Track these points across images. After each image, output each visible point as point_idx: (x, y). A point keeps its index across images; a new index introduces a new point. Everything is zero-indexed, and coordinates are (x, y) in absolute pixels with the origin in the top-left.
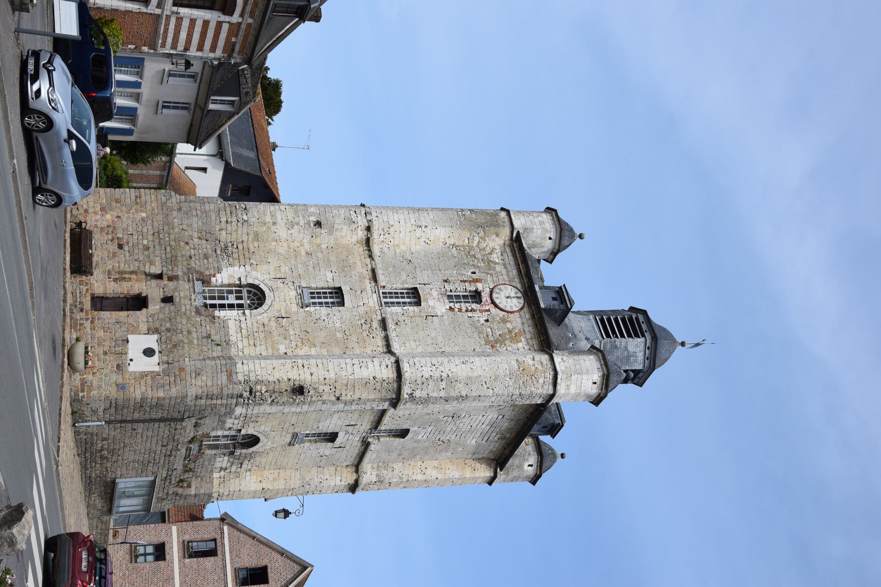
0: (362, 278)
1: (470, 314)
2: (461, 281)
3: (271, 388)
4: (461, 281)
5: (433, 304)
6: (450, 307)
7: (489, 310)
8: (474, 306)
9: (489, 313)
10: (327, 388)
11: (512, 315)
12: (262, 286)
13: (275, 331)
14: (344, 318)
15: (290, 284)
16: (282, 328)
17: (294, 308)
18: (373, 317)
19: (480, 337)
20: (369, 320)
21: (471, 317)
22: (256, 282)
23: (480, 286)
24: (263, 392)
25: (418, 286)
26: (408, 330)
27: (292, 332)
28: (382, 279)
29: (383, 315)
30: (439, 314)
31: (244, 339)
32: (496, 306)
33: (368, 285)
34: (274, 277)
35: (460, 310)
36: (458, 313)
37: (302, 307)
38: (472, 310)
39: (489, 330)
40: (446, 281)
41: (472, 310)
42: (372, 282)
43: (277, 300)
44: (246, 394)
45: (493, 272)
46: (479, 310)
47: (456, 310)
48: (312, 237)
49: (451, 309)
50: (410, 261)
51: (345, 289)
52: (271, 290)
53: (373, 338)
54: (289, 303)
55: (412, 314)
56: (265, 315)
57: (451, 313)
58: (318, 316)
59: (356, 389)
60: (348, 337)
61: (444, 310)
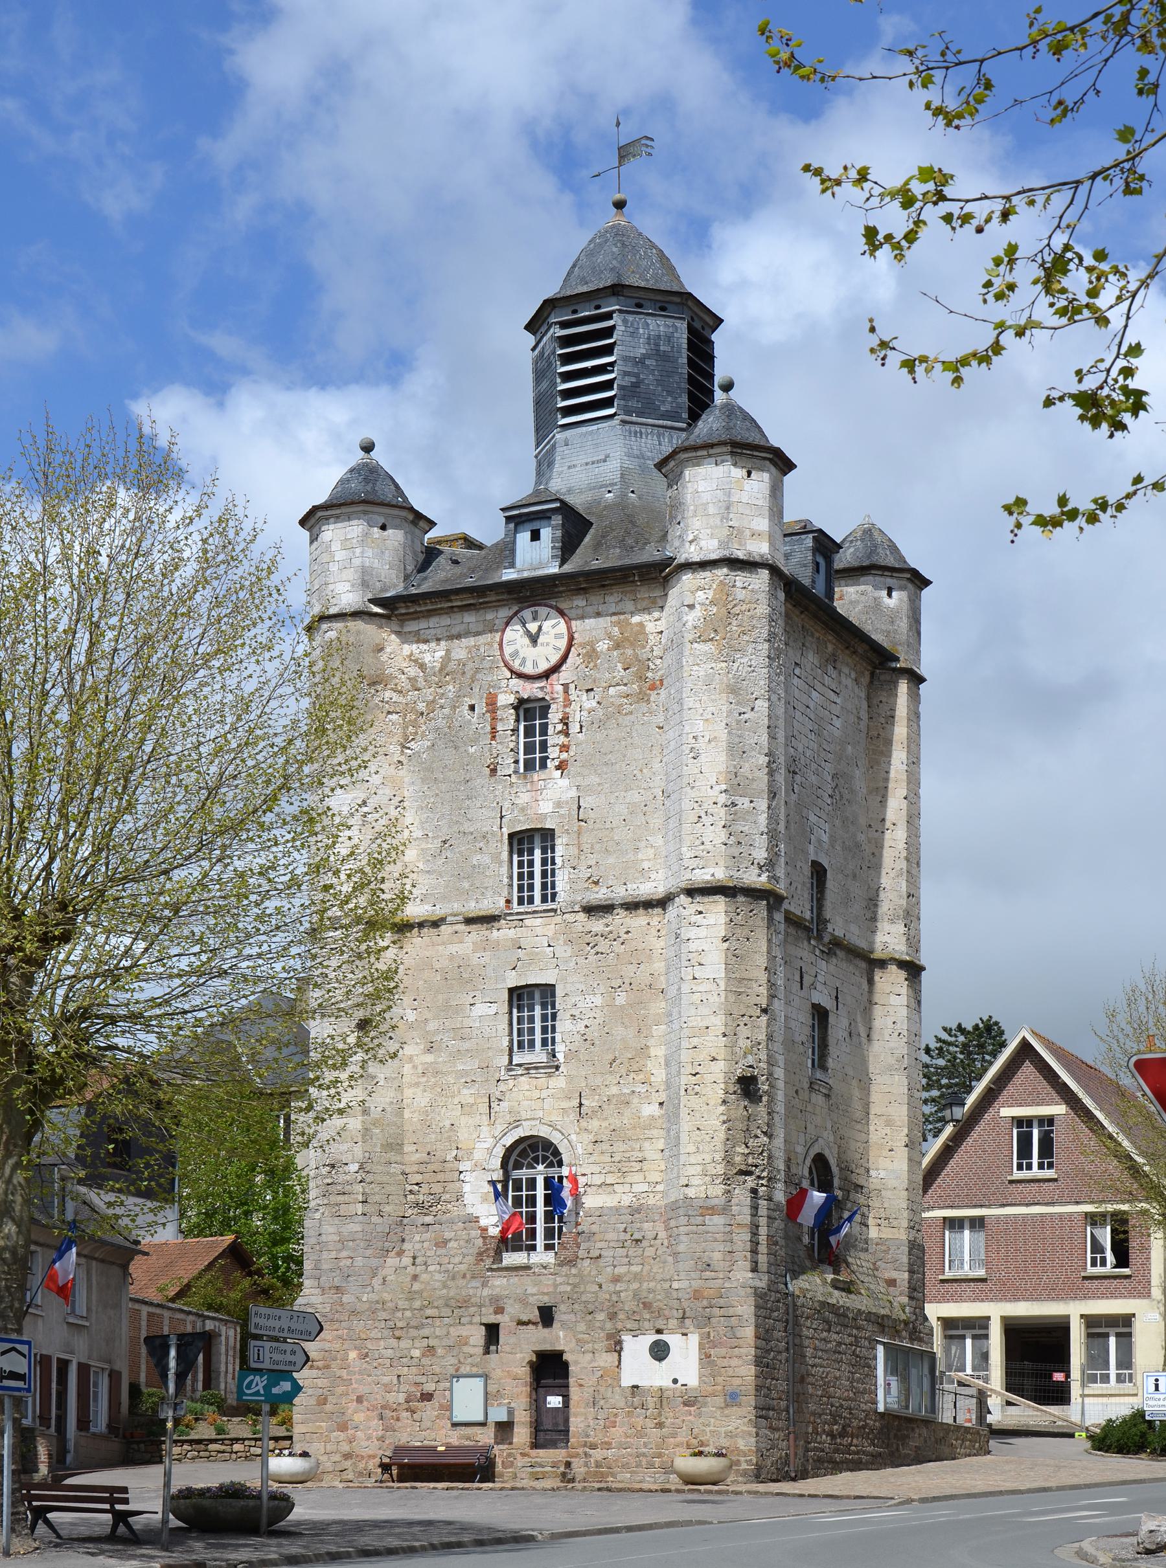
0: (485, 945)
1: (574, 728)
2: (493, 738)
3: (740, 1136)
4: (493, 738)
5: (551, 804)
6: (558, 768)
7: (566, 687)
8: (554, 716)
9: (572, 686)
10: (744, 1032)
11: (576, 636)
12: (509, 1141)
13: (611, 1120)
14: (582, 987)
15: (502, 1087)
16: (605, 1106)
17: (559, 1082)
18: (581, 929)
19: (631, 713)
20: (588, 938)
21: (581, 727)
22: (500, 1152)
23: (506, 699)
24: (747, 1151)
25: (506, 831)
26: (611, 860)
27: (614, 1090)
28: (492, 903)
29: (577, 908)
30: (573, 793)
31: (628, 1180)
32: (555, 669)
33: (503, 933)
34: (485, 1118)
35: (565, 748)
36: (572, 753)
37: (557, 1068)
38: (565, 721)
39: (612, 691)
40: (494, 771)
41: (565, 721)
42: (496, 924)
43: (540, 1114)
44: (750, 1182)
45: (470, 665)
46: (565, 706)
47: (564, 756)
48: (391, 1038)
49: (561, 767)
50: (445, 842)
51: (513, 980)
52: (516, 1124)
53: (628, 932)
54: (544, 1094)
55: (574, 851)
56: (573, 1137)
57: (572, 768)
58: (578, 1037)
59: (746, 975)
60: (627, 981)
61: (564, 782)
